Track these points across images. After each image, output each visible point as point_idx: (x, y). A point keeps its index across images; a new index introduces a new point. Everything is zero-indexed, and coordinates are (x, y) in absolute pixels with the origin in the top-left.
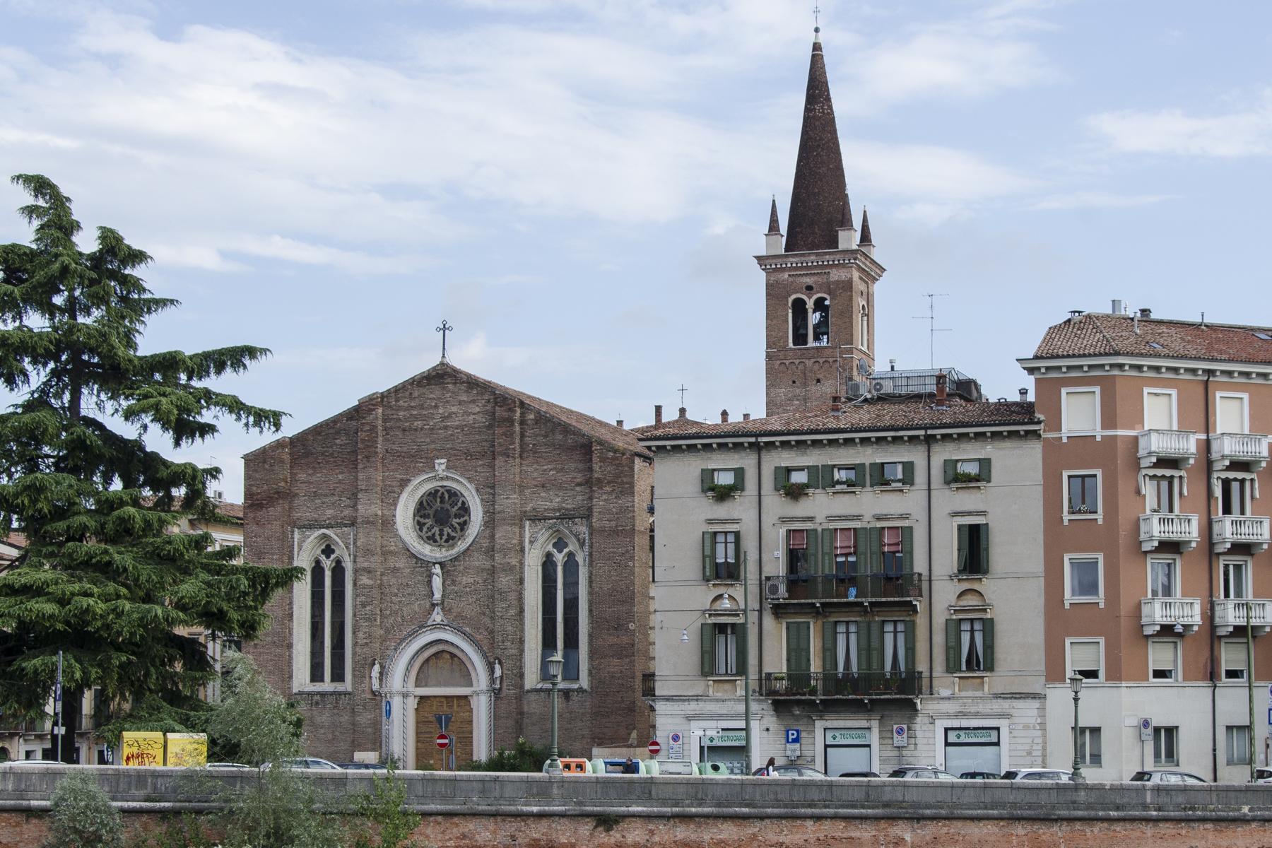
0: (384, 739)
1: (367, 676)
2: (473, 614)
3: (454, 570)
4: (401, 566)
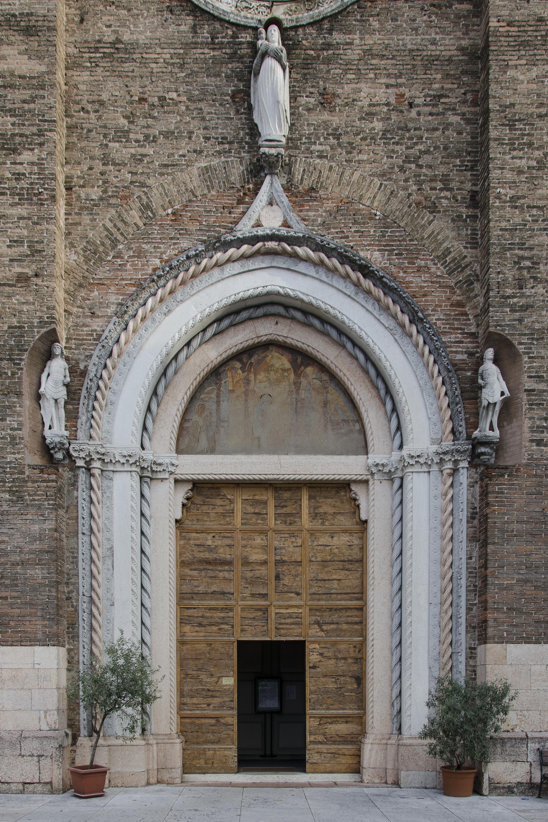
0: (83, 605)
1: (27, 389)
2: (395, 204)
3: (328, 61)
4: (142, 39)
